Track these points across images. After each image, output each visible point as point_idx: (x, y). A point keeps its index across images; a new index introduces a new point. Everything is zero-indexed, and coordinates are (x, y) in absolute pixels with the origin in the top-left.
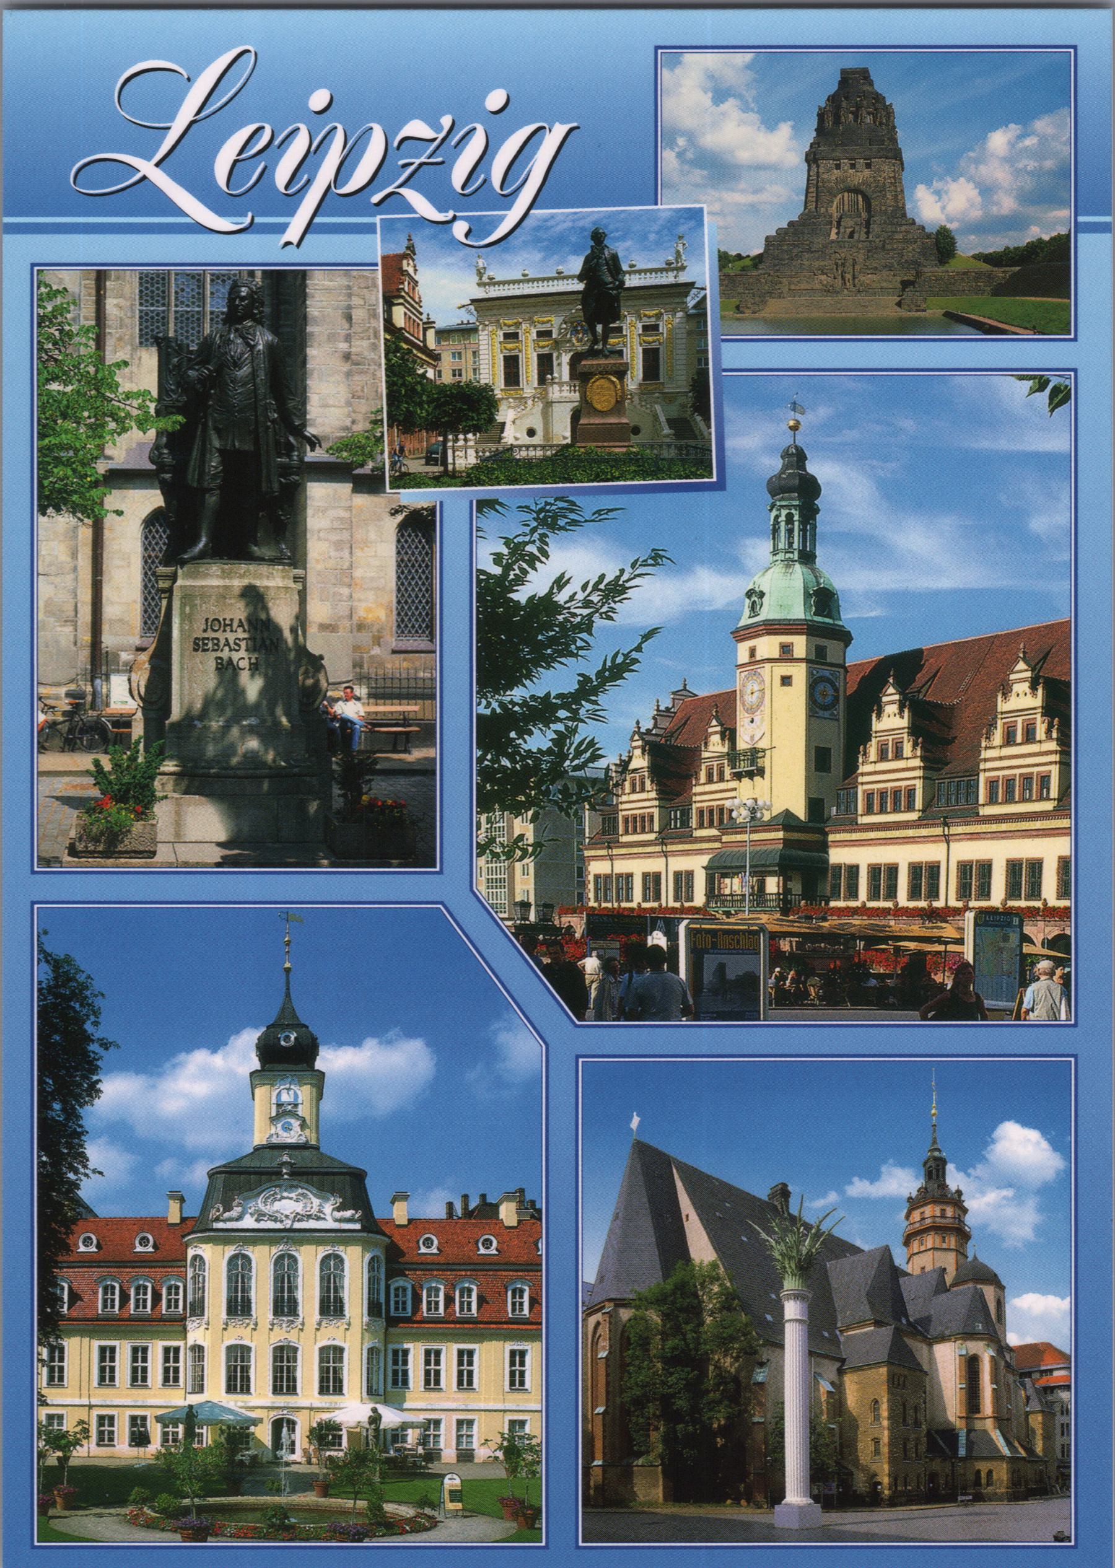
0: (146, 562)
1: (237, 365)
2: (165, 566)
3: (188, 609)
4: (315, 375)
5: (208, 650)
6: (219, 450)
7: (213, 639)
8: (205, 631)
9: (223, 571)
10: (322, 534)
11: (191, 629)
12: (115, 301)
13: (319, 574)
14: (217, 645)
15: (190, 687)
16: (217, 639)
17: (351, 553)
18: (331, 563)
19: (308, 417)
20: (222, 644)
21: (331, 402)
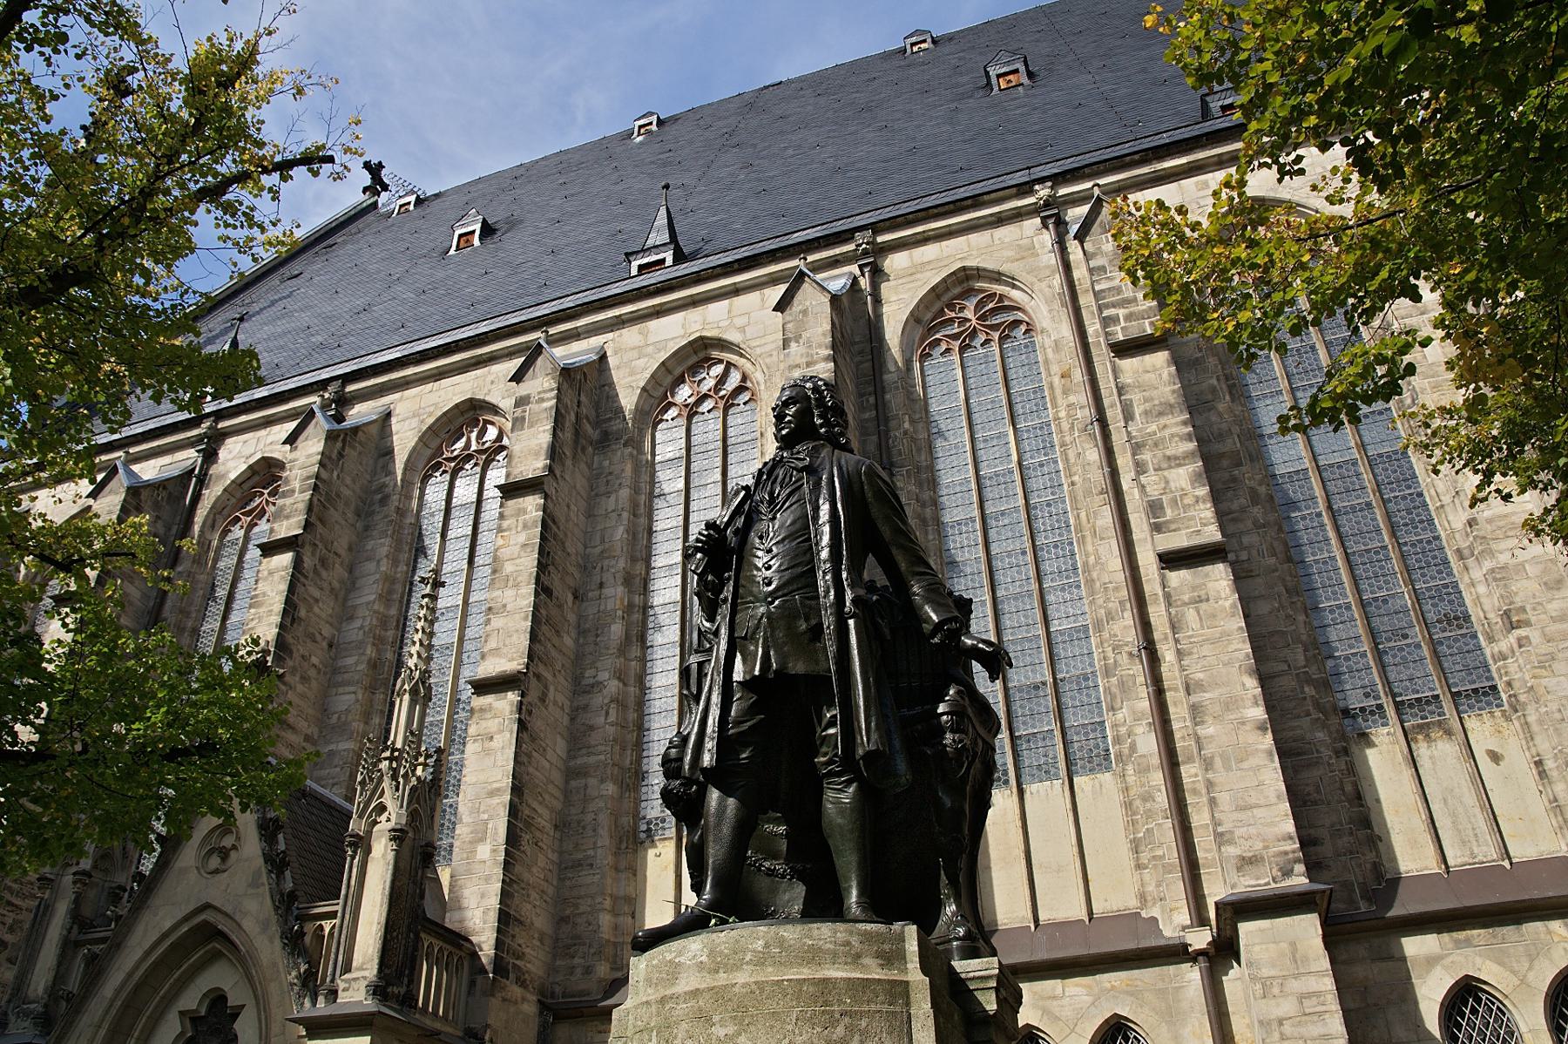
4: (1218, 762)
6: (749, 684)
9: (712, 954)
10: (1287, 1028)
21: (1253, 801)
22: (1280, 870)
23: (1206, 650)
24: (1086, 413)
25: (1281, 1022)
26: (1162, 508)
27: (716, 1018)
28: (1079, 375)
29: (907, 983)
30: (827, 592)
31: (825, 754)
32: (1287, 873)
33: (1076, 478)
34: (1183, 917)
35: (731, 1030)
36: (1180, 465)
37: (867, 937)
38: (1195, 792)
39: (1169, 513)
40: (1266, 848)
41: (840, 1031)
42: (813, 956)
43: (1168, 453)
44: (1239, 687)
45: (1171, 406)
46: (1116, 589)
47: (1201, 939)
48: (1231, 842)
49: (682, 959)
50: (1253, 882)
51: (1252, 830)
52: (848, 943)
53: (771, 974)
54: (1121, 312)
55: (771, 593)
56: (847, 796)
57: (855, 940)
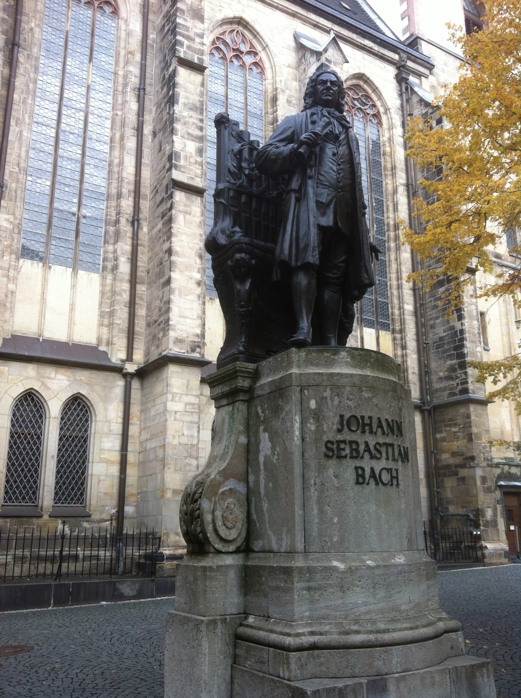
0: (12, 436)
2: (441, 287)
3: (313, 404)
4: (177, 293)
5: (345, 457)
7: (351, 443)
8: (340, 431)
10: (178, 416)
11: (319, 431)
12: (7, 217)
13: (174, 447)
14: (357, 450)
15: (321, 511)
16: (357, 443)
17: (199, 431)
18: (184, 440)
19: (170, 323)
20: (362, 447)
21: (187, 315)
22: (191, 348)
23: (184, 238)
24: (134, 80)
25: (176, 413)
26: (180, 158)
27: (364, 389)
28: (138, 57)
32: (193, 350)
33: (119, 113)
34: (123, 355)
35: (370, 395)
36: (193, 140)
38: (142, 299)
39: (182, 162)
40: (187, 337)
43: (189, 131)
44: (194, 262)
45: (197, 108)
46: (128, 183)
47: (131, 368)
48: (174, 330)
50: (179, 350)
51: (184, 328)
54: (186, 42)
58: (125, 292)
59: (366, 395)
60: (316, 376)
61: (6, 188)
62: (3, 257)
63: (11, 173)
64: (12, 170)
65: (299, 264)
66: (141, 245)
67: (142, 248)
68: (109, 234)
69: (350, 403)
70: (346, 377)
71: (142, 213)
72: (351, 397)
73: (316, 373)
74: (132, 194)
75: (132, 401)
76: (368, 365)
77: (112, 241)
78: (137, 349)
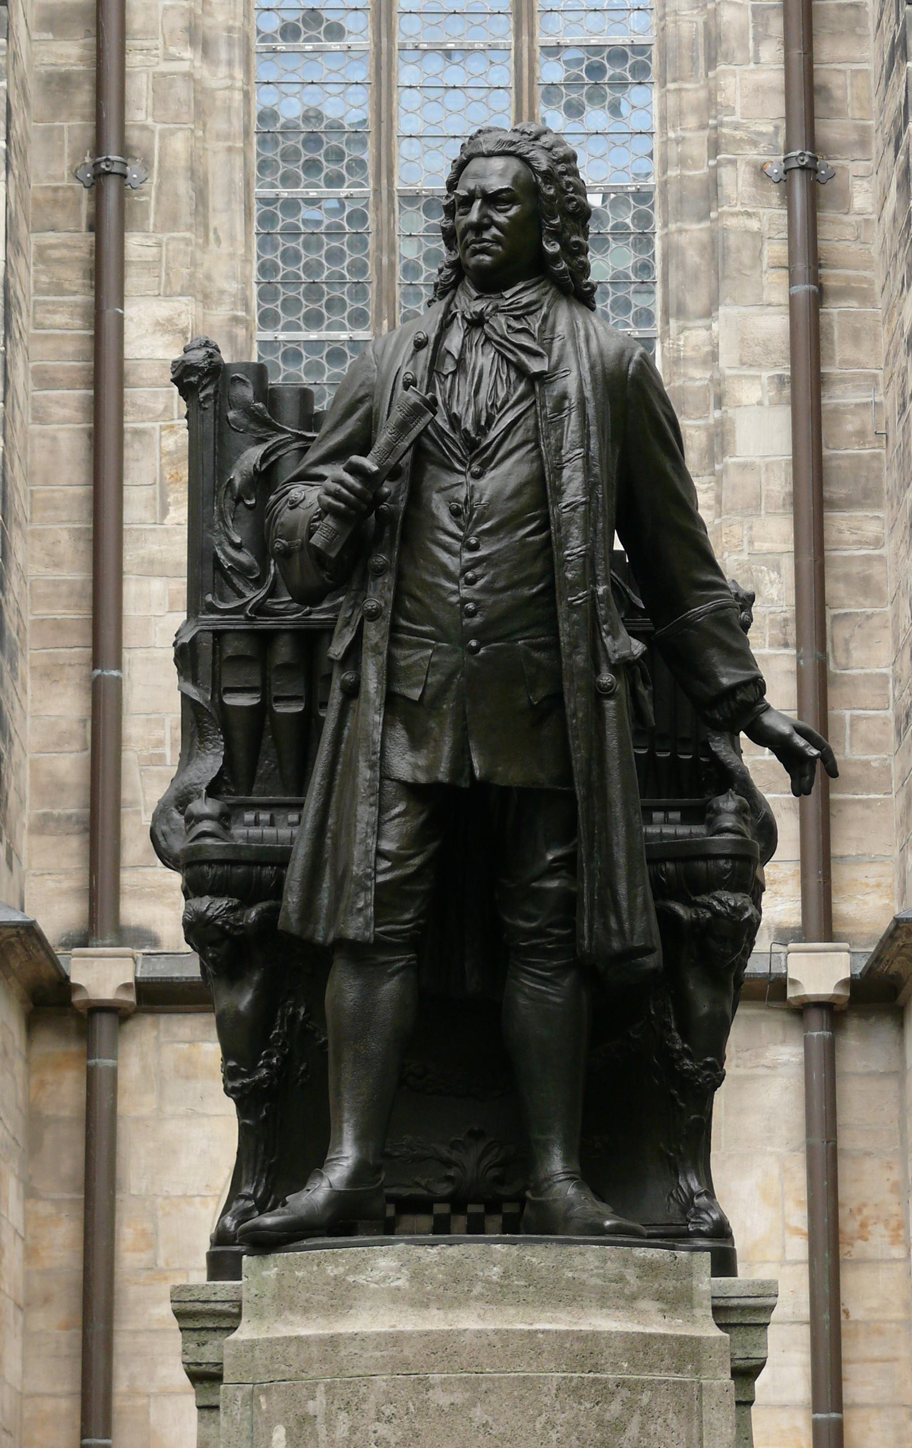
1: (477, 452)
6: (413, 791)
9: (417, 1276)
12: (162, 309)
29: (699, 1340)
30: (574, 646)
31: (529, 918)
35: (459, 1397)
37: (649, 1269)
41: (615, 1408)
42: (570, 1295)
47: (819, 973)
49: (361, 1279)
52: (621, 1279)
53: (515, 1320)
55: (476, 633)
56: (557, 994)
57: (631, 1275)
58: (777, 568)
59: (441, 1398)
60: (293, 1349)
61: (147, 164)
62: (165, 511)
63: (161, 81)
64: (165, 67)
65: (331, 937)
66: (844, 293)
67: (851, 305)
68: (682, 265)
69: (383, 1429)
70: (376, 1348)
71: (840, 113)
72: (388, 1410)
73: (289, 1340)
74: (776, 25)
75: (848, 1141)
76: (478, 1289)
77: (696, 301)
78: (858, 860)
